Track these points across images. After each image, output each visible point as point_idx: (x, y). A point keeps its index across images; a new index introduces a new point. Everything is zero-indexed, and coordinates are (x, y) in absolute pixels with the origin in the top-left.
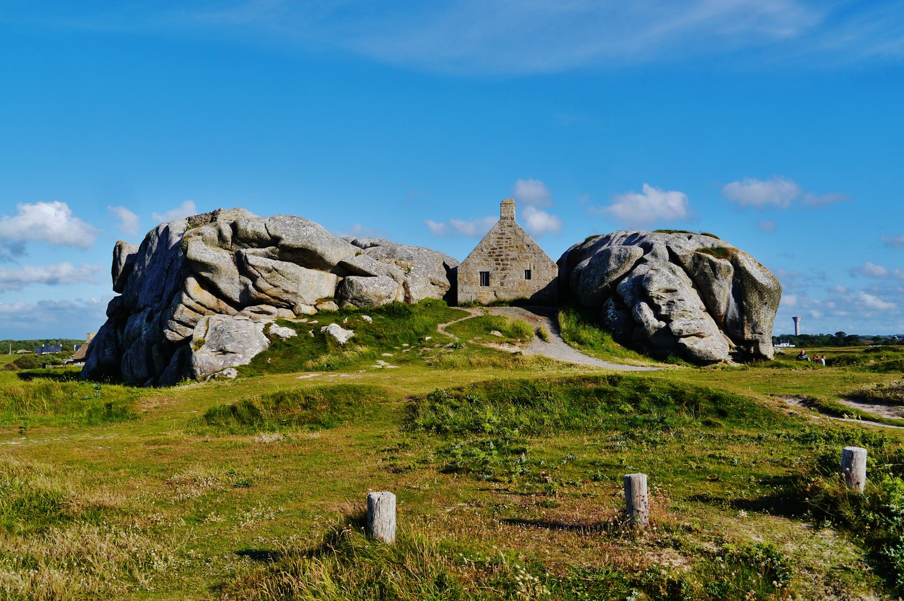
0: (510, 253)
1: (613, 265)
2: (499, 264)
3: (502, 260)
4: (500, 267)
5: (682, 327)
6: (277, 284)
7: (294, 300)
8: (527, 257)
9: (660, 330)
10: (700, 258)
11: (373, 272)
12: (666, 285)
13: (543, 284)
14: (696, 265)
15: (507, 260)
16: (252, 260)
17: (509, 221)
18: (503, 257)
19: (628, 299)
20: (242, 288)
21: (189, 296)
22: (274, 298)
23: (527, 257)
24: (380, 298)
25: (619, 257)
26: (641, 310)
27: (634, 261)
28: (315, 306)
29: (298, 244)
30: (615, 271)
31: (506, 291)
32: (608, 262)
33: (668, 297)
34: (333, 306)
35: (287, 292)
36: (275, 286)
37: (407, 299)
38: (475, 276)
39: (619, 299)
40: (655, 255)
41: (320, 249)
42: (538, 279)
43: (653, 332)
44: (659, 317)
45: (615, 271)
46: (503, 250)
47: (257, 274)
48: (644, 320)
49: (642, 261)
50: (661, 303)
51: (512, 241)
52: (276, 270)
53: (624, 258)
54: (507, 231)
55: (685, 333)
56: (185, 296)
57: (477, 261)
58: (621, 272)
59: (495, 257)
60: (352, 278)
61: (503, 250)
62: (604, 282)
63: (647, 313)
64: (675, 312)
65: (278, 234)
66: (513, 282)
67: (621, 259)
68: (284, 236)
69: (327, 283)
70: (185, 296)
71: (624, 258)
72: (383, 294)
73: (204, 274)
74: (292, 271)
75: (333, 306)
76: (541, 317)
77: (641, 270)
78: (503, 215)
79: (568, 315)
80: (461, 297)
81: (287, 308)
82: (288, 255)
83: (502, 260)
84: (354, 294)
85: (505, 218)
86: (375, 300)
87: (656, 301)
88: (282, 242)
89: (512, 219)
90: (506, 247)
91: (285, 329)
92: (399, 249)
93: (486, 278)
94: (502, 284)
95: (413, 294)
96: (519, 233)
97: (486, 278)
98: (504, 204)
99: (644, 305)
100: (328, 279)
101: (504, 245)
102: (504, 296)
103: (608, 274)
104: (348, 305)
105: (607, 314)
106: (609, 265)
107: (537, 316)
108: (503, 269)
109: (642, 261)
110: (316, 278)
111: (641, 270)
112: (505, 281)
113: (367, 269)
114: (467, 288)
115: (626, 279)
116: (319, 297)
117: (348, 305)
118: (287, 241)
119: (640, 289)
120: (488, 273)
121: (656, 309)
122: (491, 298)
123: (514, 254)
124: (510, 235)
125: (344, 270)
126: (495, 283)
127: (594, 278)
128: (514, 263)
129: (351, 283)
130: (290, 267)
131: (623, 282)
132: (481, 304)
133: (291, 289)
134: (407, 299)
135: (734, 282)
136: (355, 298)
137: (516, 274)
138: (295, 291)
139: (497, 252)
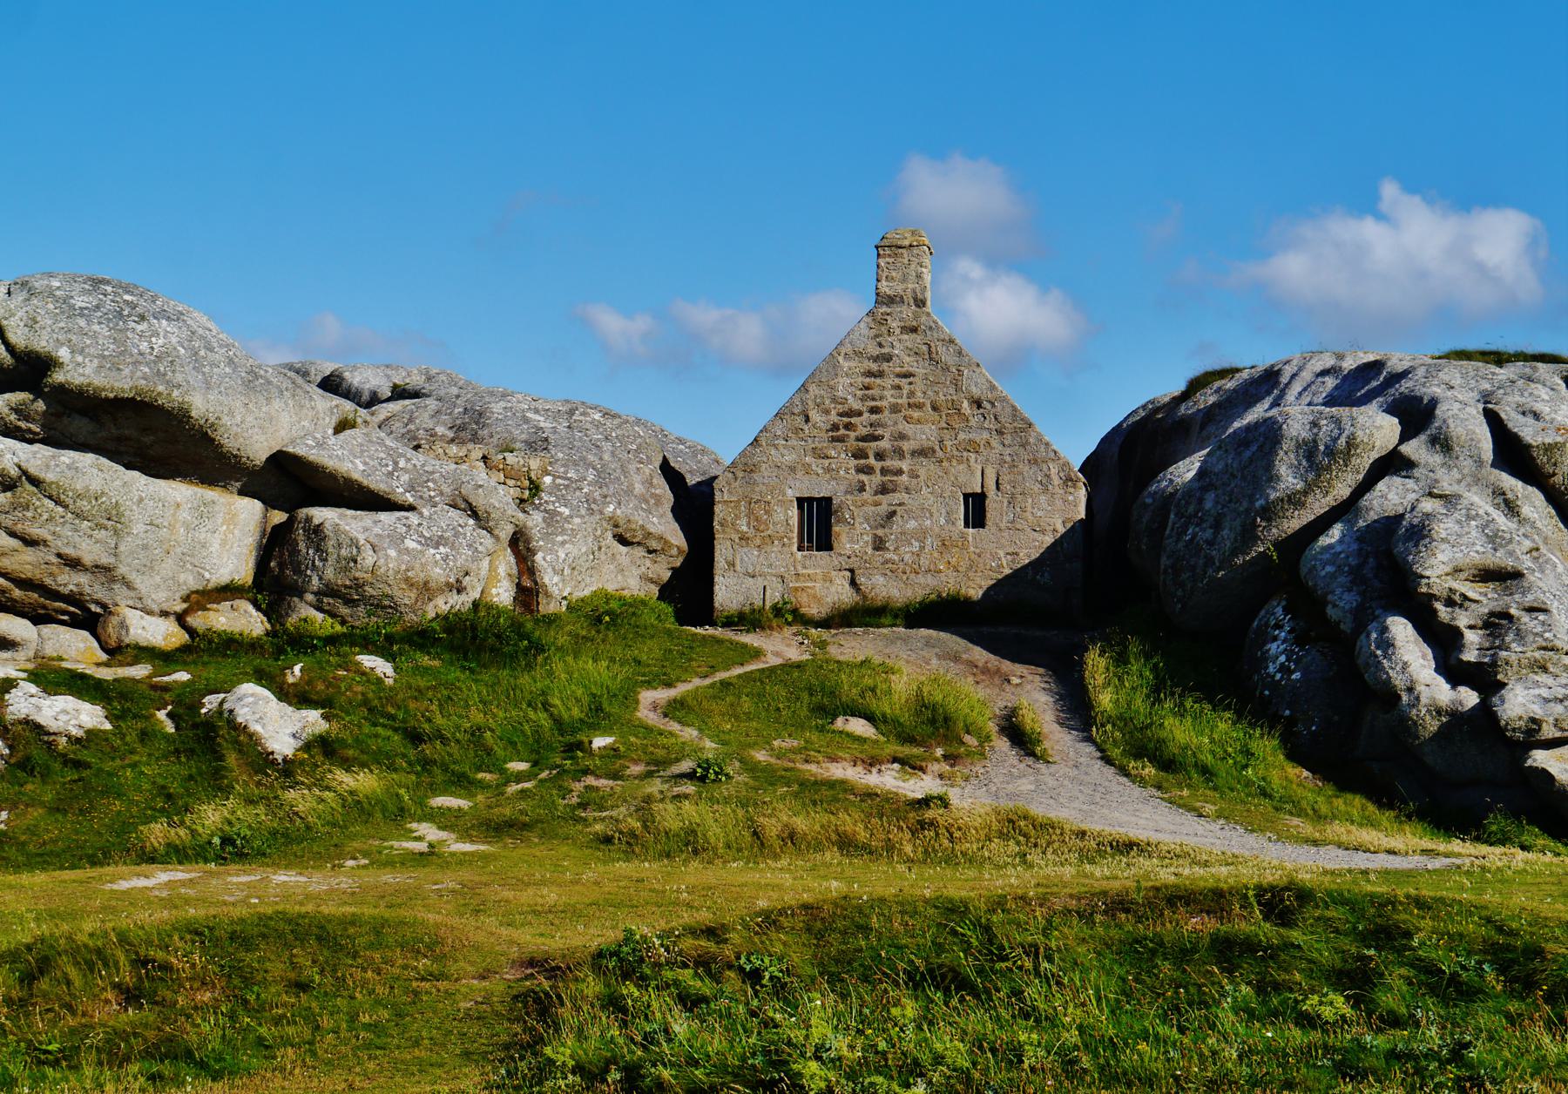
0: (908, 429)
1: (1288, 477)
2: (868, 470)
3: (880, 456)
5: (1537, 710)
6: (35, 531)
7: (100, 593)
8: (973, 447)
9: (1456, 720)
11: (401, 493)
12: (1478, 553)
13: (1031, 547)
15: (901, 454)
17: (907, 312)
18: (885, 444)
19: (1341, 603)
22: (25, 584)
23: (973, 447)
24: (426, 590)
25: (1309, 450)
26: (1387, 645)
27: (1364, 461)
28: (181, 619)
29: (121, 383)
30: (1295, 501)
31: (890, 569)
32: (1270, 466)
33: (1486, 598)
34: (247, 620)
35: (74, 564)
36: (30, 542)
37: (528, 593)
38: (779, 515)
40: (1442, 443)
41: (200, 405)
42: (1013, 526)
43: (1432, 725)
44: (1454, 671)
45: (1295, 501)
46: (886, 416)
48: (1399, 681)
49: (1393, 464)
50: (1462, 620)
51: (919, 386)
52: (35, 482)
53: (1331, 452)
54: (900, 346)
55: (1548, 732)
57: (789, 458)
58: (1319, 505)
59: (852, 443)
60: (322, 515)
61: (886, 416)
62: (1255, 539)
63: (1409, 656)
64: (1514, 652)
65: (42, 343)
66: (922, 535)
67: (1319, 458)
68: (63, 354)
69: (222, 533)
71: (1331, 452)
72: (438, 574)
74: (96, 485)
75: (247, 620)
76: (1020, 669)
77: (1391, 496)
78: (885, 287)
79: (1121, 660)
80: (728, 592)
81: (75, 623)
82: (80, 426)
83: (880, 456)
84: (329, 573)
85: (891, 300)
86: (406, 598)
87: (1443, 612)
88: (58, 377)
89: (920, 303)
90: (895, 409)
91: (65, 702)
92: (497, 408)
93: (818, 522)
94: (879, 544)
95: (549, 579)
96: (946, 355)
97: (818, 522)
98: (888, 248)
99: (1401, 629)
100: (231, 519)
101: (890, 398)
102: (883, 588)
103: (1270, 513)
104: (306, 614)
105: (1265, 659)
106: (1273, 478)
107: (1006, 665)
108: (883, 490)
109: (1393, 464)
110: (184, 515)
111: (1391, 496)
112: (891, 534)
113: (377, 483)
114: (749, 557)
115: (1336, 532)
116: (191, 582)
117: (306, 614)
118: (79, 369)
119: (1387, 566)
120: (828, 501)
121: (1443, 641)
122: (839, 593)
123: (924, 433)
124: (910, 364)
125: (290, 482)
126: (851, 539)
127: (1217, 526)
128: (926, 468)
129: (316, 533)
130: (86, 471)
131: (1324, 541)
132: (801, 620)
133: (89, 551)
134: (528, 593)
136: (329, 591)
137: (931, 506)
138: (105, 560)
139: (862, 425)
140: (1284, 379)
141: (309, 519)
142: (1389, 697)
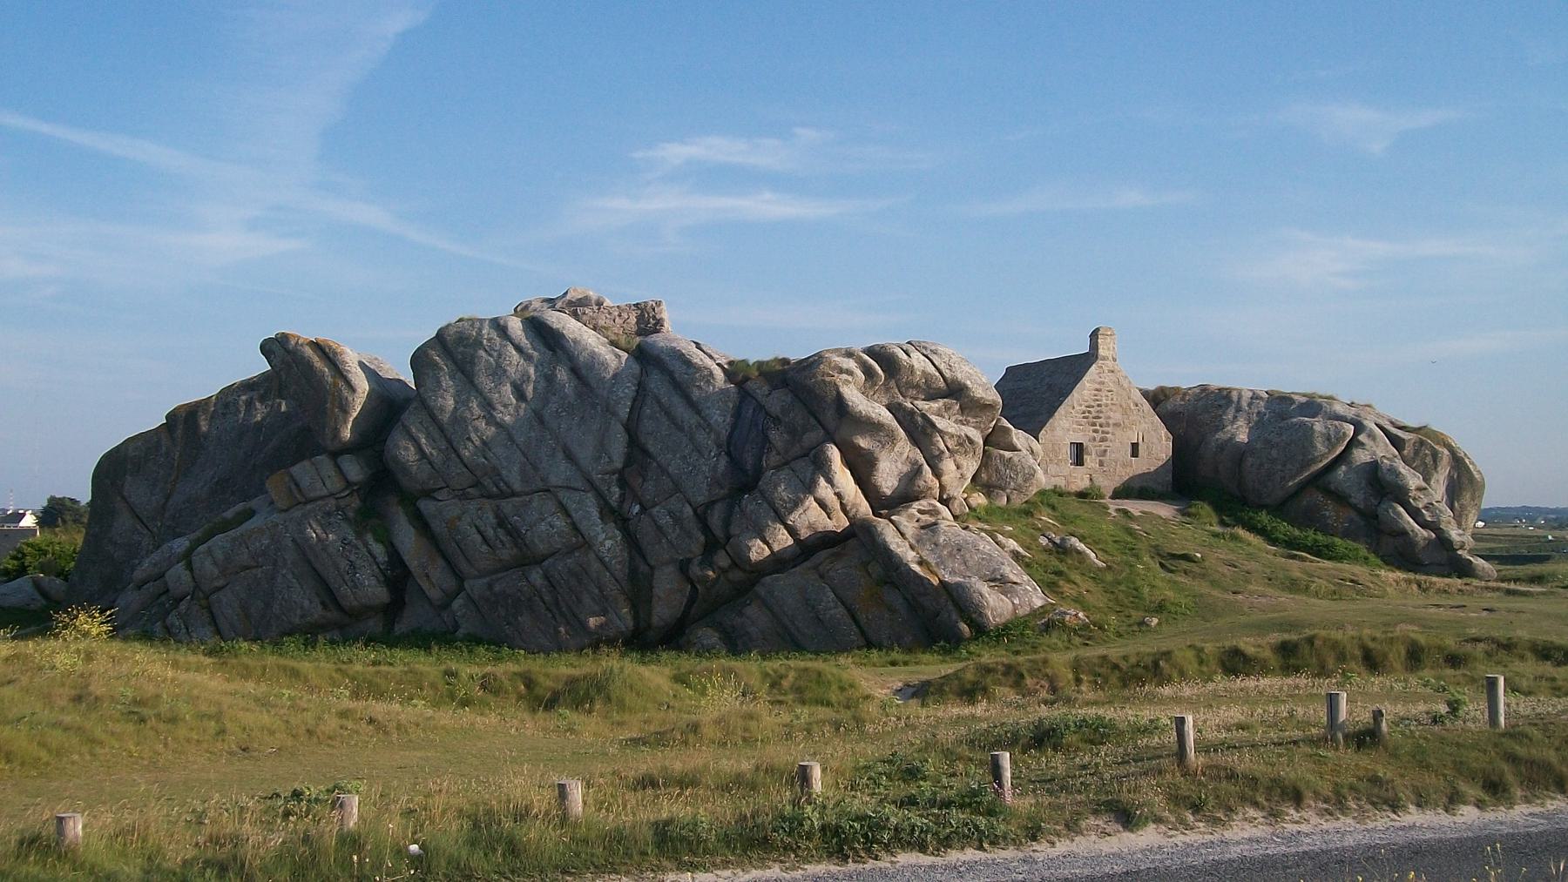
1: (1321, 447)
4: (1098, 436)
9: (1430, 541)
10: (1422, 443)
14: (1416, 453)
16: (941, 423)
19: (1358, 498)
20: (906, 469)
21: (830, 481)
26: (1399, 514)
39: (1340, 498)
40: (1372, 436)
43: (1422, 543)
44: (1424, 525)
47: (942, 446)
49: (1354, 443)
56: (822, 481)
67: (1330, 441)
70: (822, 481)
73: (863, 442)
94: (1101, 464)
103: (1314, 461)
108: (1103, 440)
121: (1415, 514)
123: (1116, 416)
124: (1112, 386)
128: (1118, 432)
135: (1450, 477)
140: (1235, 398)
141: (1002, 456)
142: (1403, 533)
